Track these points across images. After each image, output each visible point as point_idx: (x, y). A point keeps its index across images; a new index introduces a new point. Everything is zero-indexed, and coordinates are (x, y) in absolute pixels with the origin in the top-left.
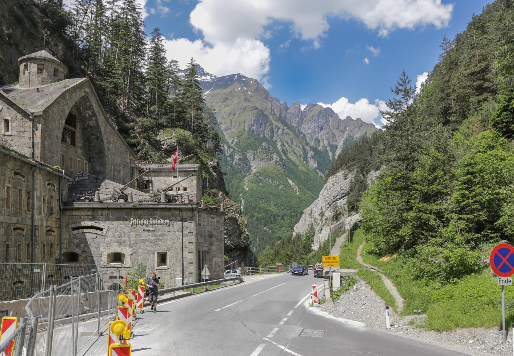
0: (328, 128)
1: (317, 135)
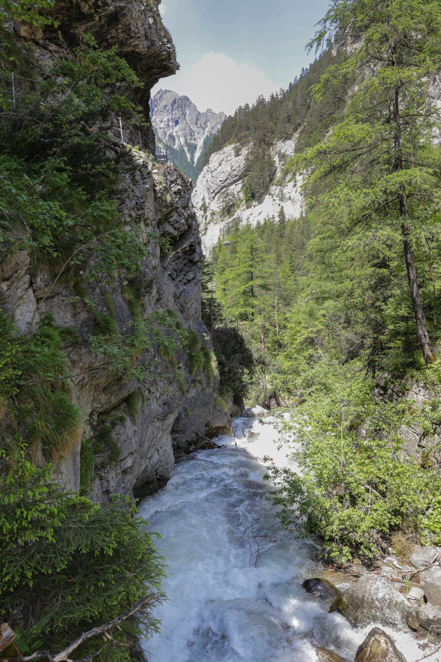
0: (185, 122)
1: (171, 131)
